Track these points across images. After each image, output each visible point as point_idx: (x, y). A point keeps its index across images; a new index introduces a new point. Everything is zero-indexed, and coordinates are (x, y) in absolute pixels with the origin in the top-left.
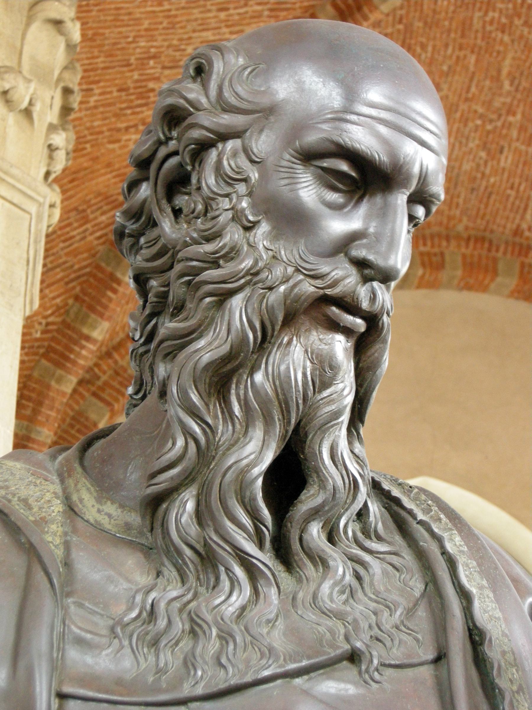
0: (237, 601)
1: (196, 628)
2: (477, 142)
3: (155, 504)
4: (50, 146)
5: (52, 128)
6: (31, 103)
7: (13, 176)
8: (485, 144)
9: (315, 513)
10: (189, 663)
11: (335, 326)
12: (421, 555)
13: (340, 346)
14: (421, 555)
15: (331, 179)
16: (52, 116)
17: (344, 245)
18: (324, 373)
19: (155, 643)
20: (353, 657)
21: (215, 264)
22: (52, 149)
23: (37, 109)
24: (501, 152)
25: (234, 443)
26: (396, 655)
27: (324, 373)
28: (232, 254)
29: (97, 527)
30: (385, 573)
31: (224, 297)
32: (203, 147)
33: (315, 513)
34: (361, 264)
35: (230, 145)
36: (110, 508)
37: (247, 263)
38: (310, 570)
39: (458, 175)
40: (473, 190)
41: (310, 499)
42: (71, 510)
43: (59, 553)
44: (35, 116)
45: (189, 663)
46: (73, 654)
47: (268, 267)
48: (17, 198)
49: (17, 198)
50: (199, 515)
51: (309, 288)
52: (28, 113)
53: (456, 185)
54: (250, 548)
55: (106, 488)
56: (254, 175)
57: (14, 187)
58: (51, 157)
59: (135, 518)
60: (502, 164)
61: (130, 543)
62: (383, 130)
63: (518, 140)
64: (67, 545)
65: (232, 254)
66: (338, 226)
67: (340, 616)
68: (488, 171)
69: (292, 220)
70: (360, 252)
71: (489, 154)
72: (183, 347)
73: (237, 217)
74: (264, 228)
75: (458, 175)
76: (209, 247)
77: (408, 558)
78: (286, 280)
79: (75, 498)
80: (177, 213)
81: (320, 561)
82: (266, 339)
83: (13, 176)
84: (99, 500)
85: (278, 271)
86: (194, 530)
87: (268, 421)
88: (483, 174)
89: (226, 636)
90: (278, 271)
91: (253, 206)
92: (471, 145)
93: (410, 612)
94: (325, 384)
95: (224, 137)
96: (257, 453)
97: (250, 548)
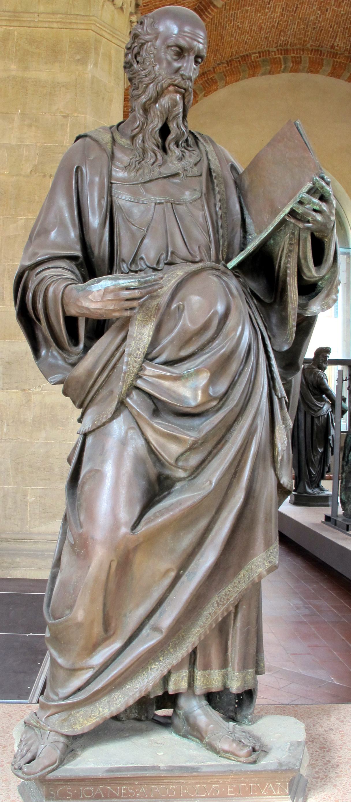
2: (317, 7)
3: (133, 138)
5: (131, 14)
6: (122, 5)
7: (117, 35)
8: (320, 7)
13: (178, 97)
16: (132, 9)
22: (131, 22)
23: (125, 6)
24: (327, 11)
27: (175, 104)
32: (143, 44)
35: (149, 44)
39: (308, 22)
40: (314, 28)
41: (171, 137)
44: (124, 10)
52: (122, 8)
53: (307, 26)
57: (118, 39)
58: (131, 26)
59: (129, 142)
60: (327, 16)
62: (187, 39)
63: (334, 5)
68: (321, 20)
71: (321, 12)
72: (139, 98)
75: (308, 22)
79: (115, 138)
80: (138, 62)
83: (117, 35)
84: (121, 138)
88: (319, 21)
92: (314, 8)
94: (175, 106)
95: (148, 42)
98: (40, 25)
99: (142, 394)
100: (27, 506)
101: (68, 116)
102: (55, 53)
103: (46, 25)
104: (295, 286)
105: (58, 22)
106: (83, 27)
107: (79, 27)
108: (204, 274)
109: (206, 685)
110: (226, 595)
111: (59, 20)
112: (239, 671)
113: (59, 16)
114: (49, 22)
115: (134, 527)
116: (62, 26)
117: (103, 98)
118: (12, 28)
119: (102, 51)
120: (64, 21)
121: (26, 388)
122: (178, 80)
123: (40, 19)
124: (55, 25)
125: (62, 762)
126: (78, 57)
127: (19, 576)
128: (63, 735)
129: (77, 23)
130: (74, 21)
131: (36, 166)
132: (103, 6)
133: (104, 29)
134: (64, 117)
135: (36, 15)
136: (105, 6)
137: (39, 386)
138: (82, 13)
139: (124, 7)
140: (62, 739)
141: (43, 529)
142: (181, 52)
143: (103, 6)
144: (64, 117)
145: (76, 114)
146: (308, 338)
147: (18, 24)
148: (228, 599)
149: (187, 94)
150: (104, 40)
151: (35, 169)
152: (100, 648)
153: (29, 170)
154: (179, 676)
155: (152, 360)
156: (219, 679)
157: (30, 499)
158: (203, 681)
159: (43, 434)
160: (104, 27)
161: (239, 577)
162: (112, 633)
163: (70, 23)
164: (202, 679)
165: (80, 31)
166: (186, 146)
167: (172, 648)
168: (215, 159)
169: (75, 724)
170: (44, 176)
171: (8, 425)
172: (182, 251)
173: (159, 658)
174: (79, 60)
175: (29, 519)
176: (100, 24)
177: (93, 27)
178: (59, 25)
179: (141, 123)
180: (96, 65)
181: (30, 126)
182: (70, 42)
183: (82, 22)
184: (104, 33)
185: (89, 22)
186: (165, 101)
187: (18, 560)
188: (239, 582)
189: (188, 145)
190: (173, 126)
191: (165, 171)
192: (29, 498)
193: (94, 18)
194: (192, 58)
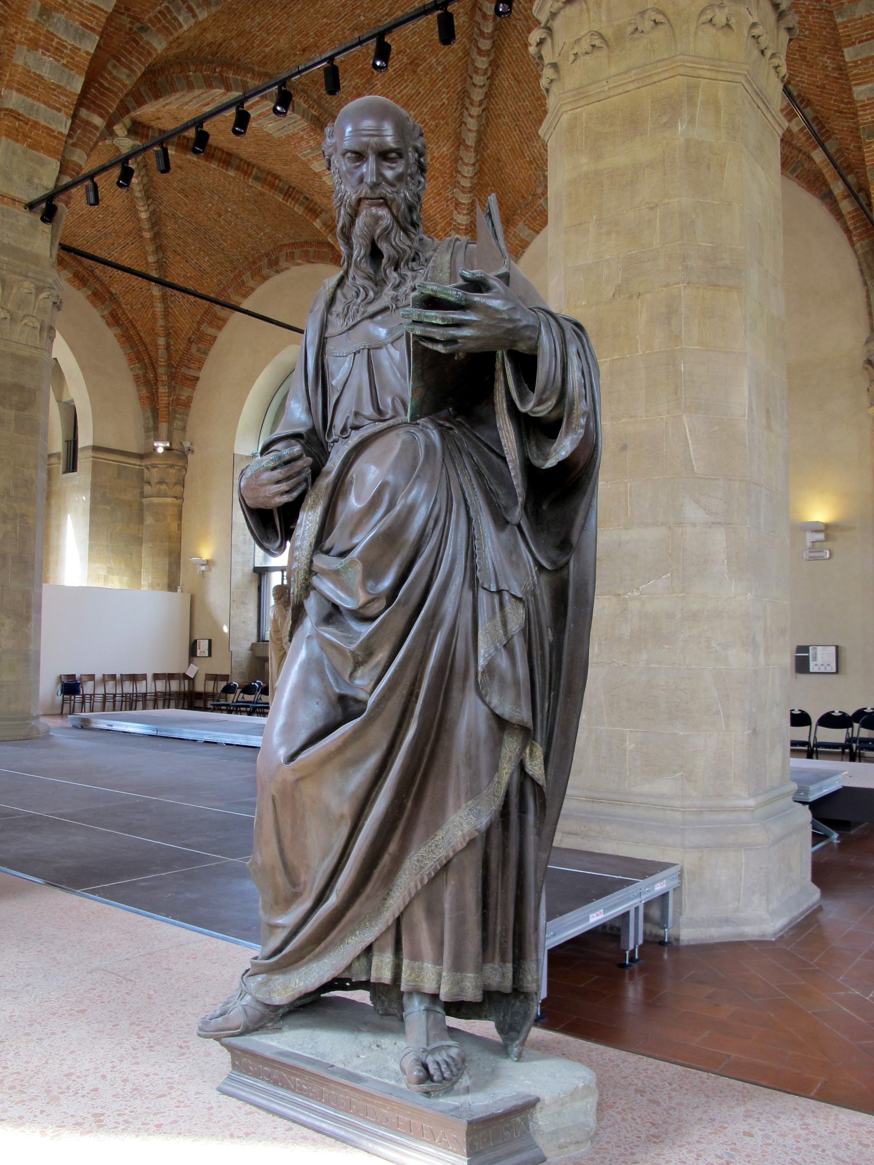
4: (753, 36)
6: (728, 20)
7: (723, 67)
44: (733, 26)
48: (730, 77)
49: (730, 77)
52: (728, 25)
57: (726, 72)
98: (612, 93)
99: (318, 596)
100: (625, 755)
101: (656, 206)
102: (633, 124)
103: (620, 90)
104: (508, 430)
105: (633, 81)
106: (667, 75)
107: (662, 76)
108: (391, 435)
109: (414, 981)
110: (418, 860)
111: (634, 78)
112: (449, 970)
113: (633, 72)
114: (622, 85)
115: (292, 758)
116: (640, 85)
117: (708, 166)
118: (579, 110)
119: (700, 98)
120: (641, 76)
121: (620, 592)
122: (365, 191)
123: (610, 86)
124: (631, 86)
125: (247, 1031)
126: (665, 119)
127: (609, 852)
128: (257, 1001)
129: (658, 73)
130: (654, 72)
131: (620, 285)
132: (696, 34)
133: (700, 66)
134: (652, 209)
135: (604, 83)
136: (700, 33)
137: (638, 589)
138: (665, 56)
139: (730, 22)
140: (260, 1008)
141: (646, 788)
142: (359, 156)
143: (696, 34)
144: (652, 209)
145: (666, 201)
146: (586, 500)
147: (584, 102)
148: (421, 868)
149: (389, 203)
150: (703, 81)
151: (618, 290)
152: (294, 906)
153: (611, 294)
154: (382, 961)
155: (327, 552)
156: (433, 977)
157: (630, 746)
158: (410, 975)
159: (644, 656)
160: (699, 63)
161: (437, 838)
162: (301, 887)
163: (650, 76)
164: (409, 972)
165: (664, 82)
167: (369, 921)
169: (274, 992)
170: (631, 297)
171: (600, 644)
172: (368, 410)
173: (355, 931)
174: (665, 123)
175: (628, 774)
176: (692, 62)
177: (682, 71)
178: (636, 85)
180: (691, 122)
181: (609, 233)
182: (652, 102)
183: (665, 68)
184: (701, 72)
185: (674, 65)
186: (360, 222)
187: (608, 828)
188: (436, 846)
190: (383, 247)
191: (372, 309)
192: (627, 743)
193: (680, 57)
194: (371, 159)
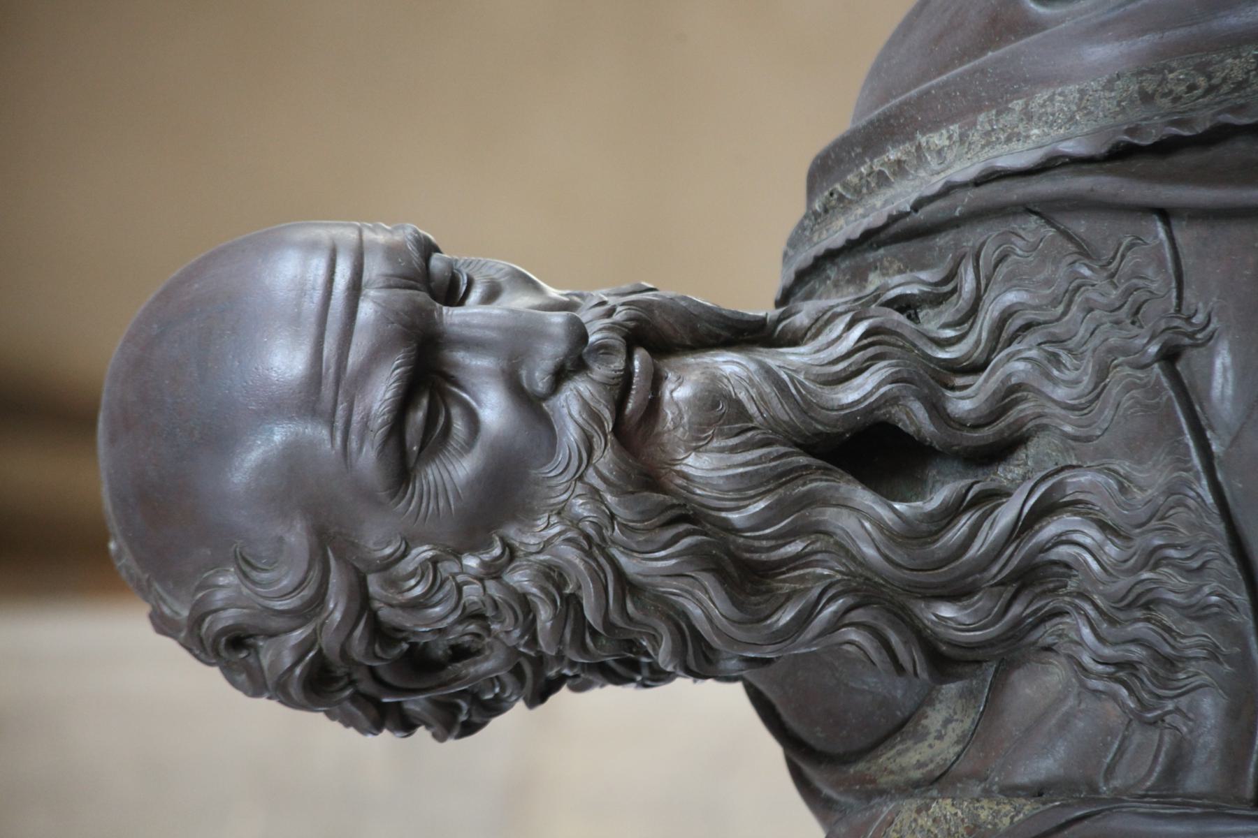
0: (1090, 535)
1: (1146, 603)
3: (944, 661)
9: (936, 409)
10: (1198, 613)
11: (653, 406)
12: (977, 215)
14: (977, 215)
15: (436, 439)
17: (529, 403)
18: (721, 414)
19: (1170, 663)
20: (1170, 356)
21: (573, 602)
25: (844, 551)
26: (1158, 281)
28: (553, 576)
29: (967, 740)
30: (1013, 281)
31: (627, 586)
32: (381, 633)
33: (936, 409)
34: (560, 376)
36: (934, 719)
37: (571, 556)
38: (1026, 408)
41: (915, 417)
42: (938, 781)
43: (1029, 807)
45: (1198, 613)
46: (1196, 781)
47: (575, 522)
50: (955, 595)
51: (605, 458)
54: (1006, 515)
55: (900, 727)
56: (423, 552)
61: (998, 686)
64: (1011, 791)
65: (553, 576)
66: (493, 408)
67: (1103, 372)
69: (504, 494)
70: (539, 379)
73: (493, 571)
74: (512, 532)
76: (545, 615)
77: (986, 237)
78: (594, 494)
81: (1010, 395)
82: (686, 514)
85: (580, 507)
86: (980, 601)
87: (810, 500)
89: (1153, 559)
90: (580, 507)
91: (473, 550)
93: (1085, 252)
96: (862, 517)
97: (1006, 515)
166: (949, 312)
168: (1028, 116)
179: (855, 616)
189: (936, 300)
